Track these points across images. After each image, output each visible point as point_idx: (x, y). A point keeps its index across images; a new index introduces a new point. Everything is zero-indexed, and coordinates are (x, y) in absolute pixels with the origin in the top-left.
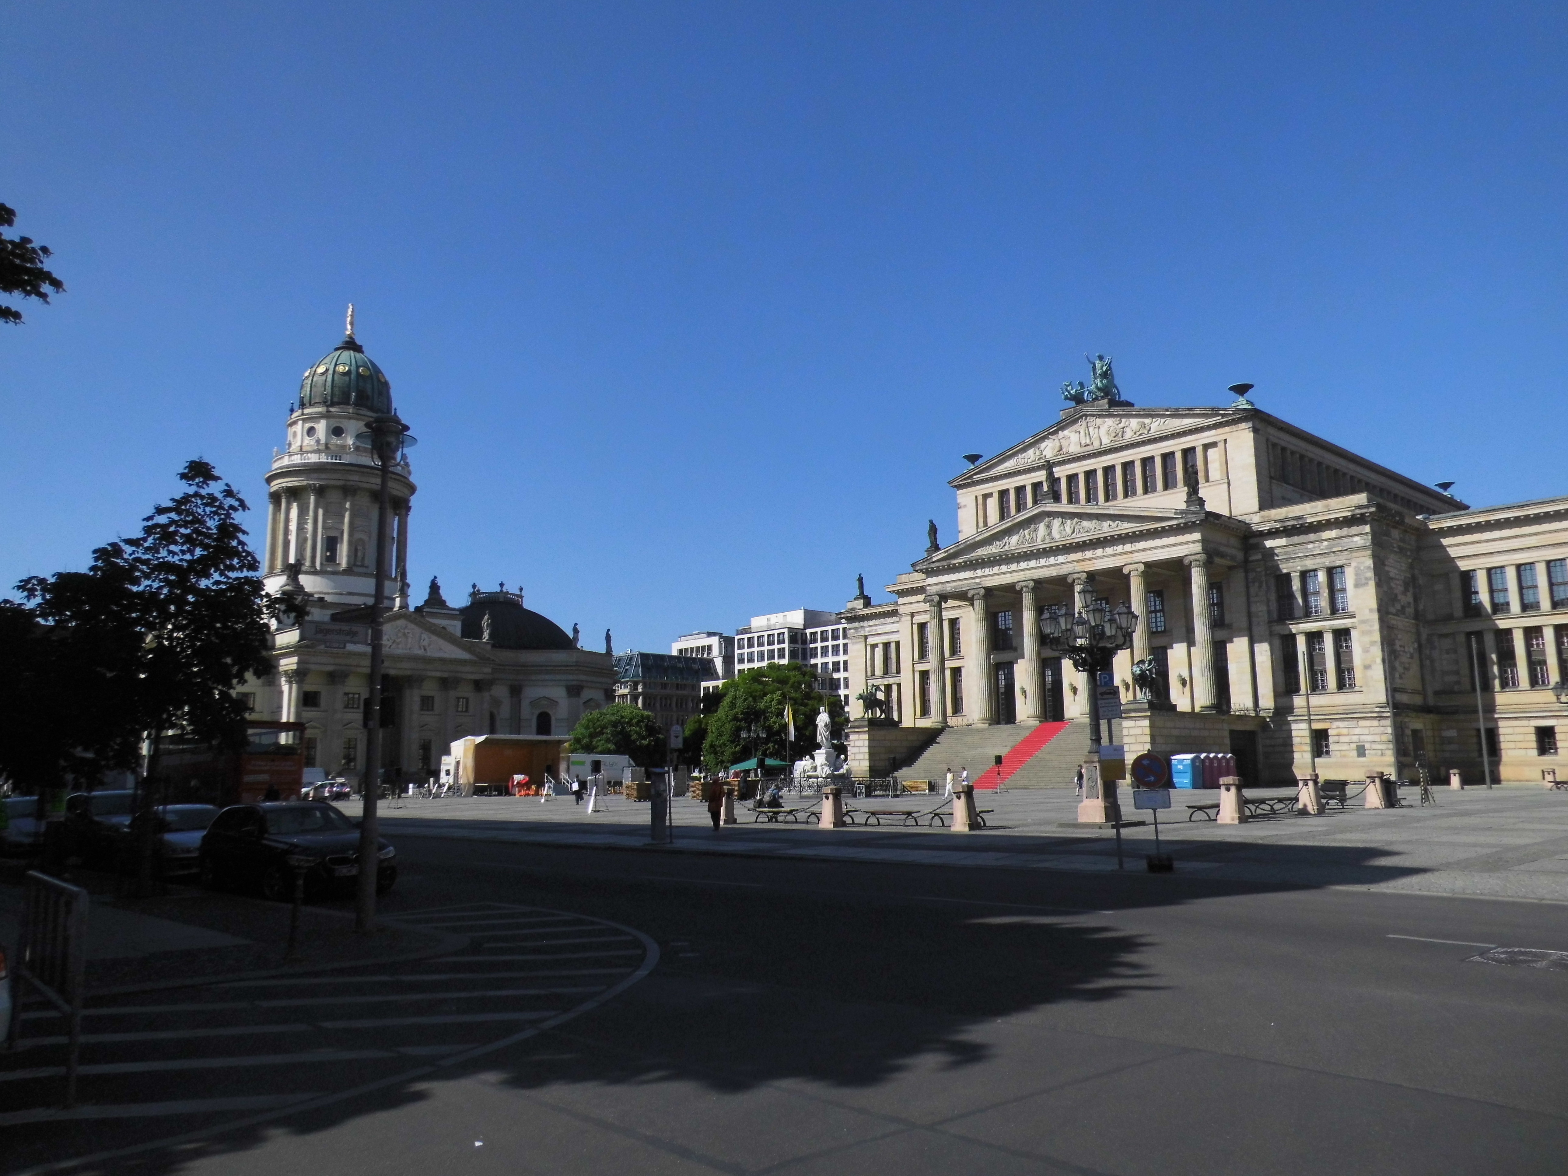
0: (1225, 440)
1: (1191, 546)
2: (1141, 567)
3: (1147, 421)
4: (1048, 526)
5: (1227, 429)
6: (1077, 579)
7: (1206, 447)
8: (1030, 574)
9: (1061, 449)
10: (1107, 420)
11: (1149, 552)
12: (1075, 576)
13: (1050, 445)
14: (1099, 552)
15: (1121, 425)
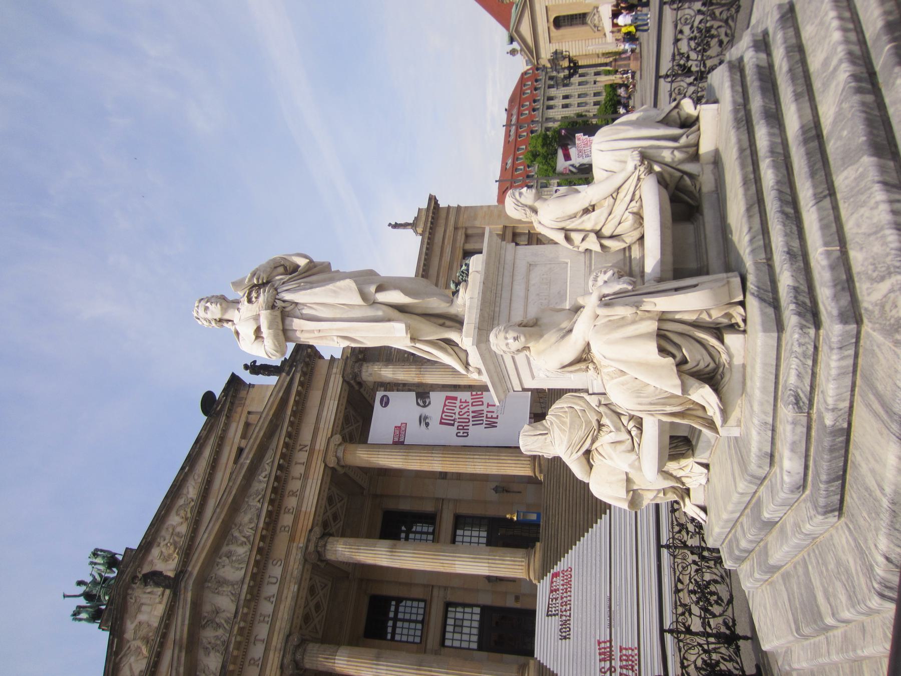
0: (249, 413)
1: (334, 370)
2: (338, 438)
3: (181, 502)
4: (222, 582)
5: (239, 409)
6: (316, 546)
7: (244, 436)
8: (277, 641)
9: (146, 640)
10: (150, 558)
11: (322, 425)
12: (311, 548)
13: (132, 659)
14: (291, 502)
15: (168, 537)
